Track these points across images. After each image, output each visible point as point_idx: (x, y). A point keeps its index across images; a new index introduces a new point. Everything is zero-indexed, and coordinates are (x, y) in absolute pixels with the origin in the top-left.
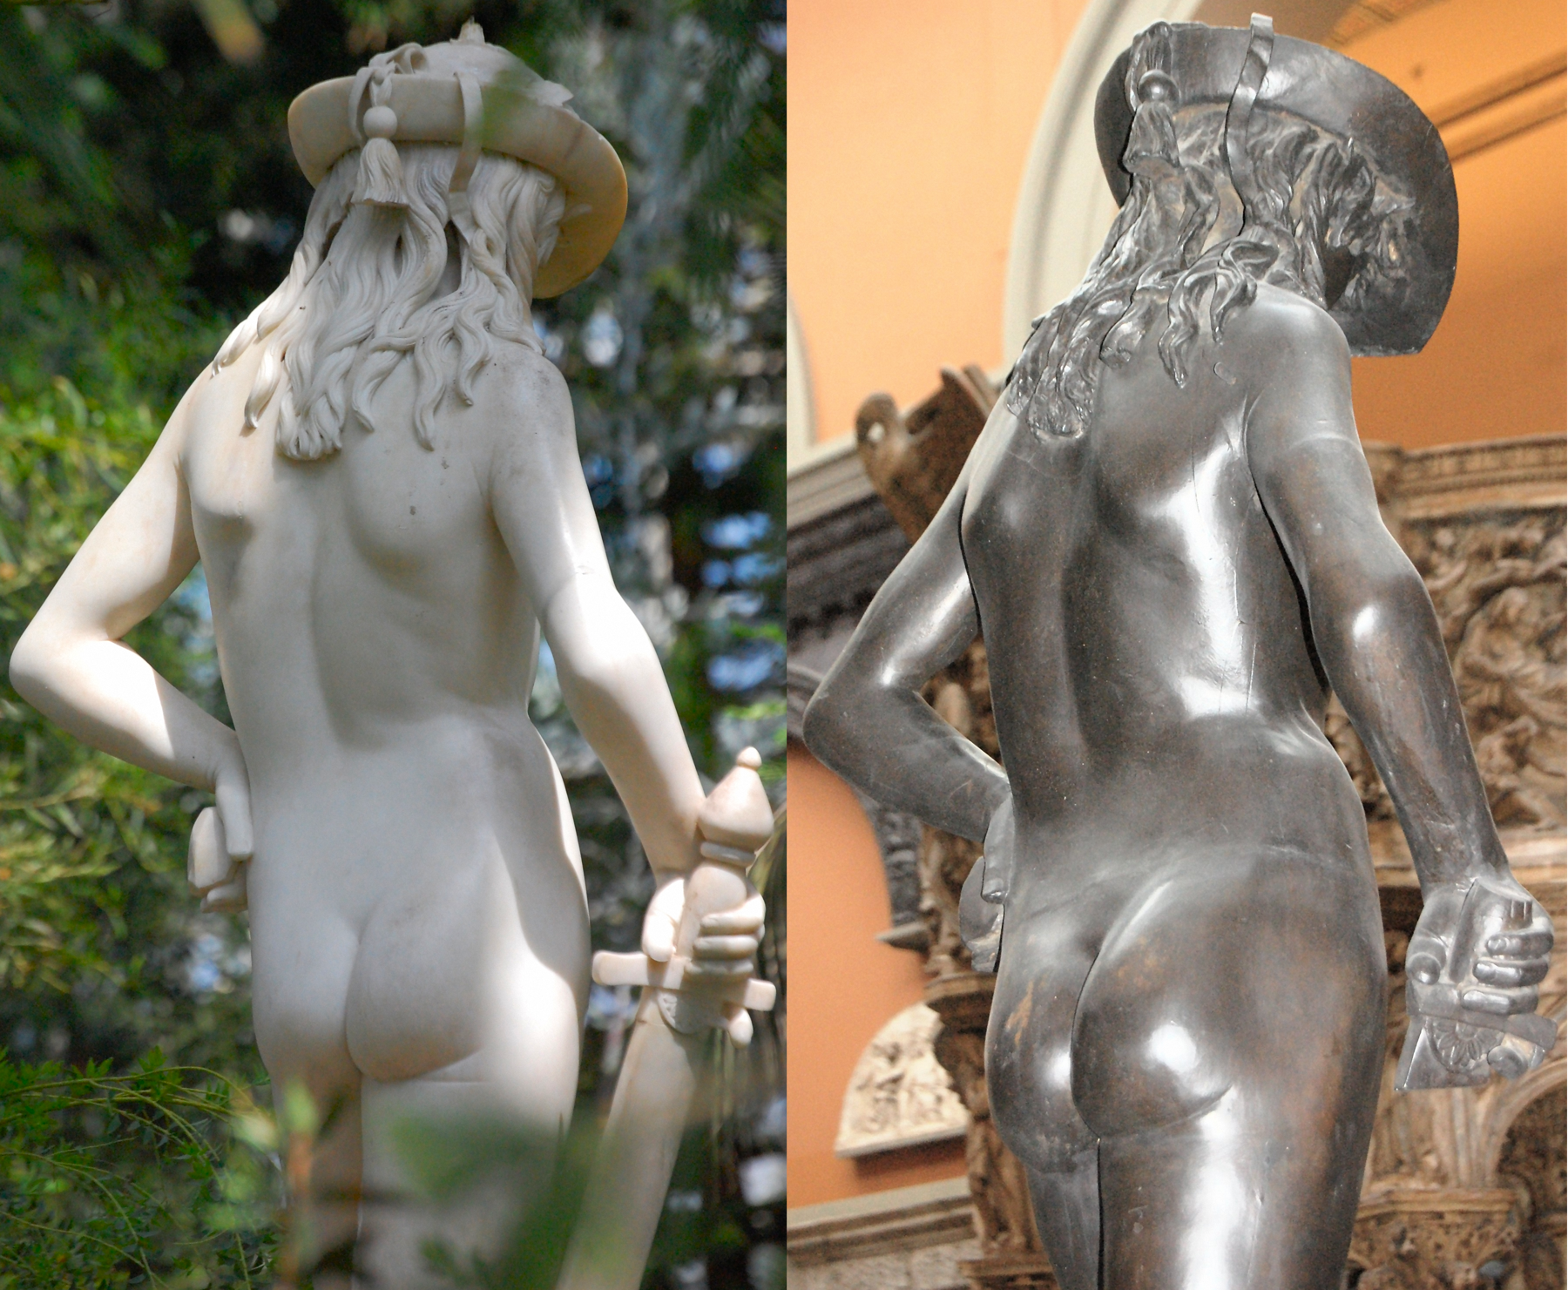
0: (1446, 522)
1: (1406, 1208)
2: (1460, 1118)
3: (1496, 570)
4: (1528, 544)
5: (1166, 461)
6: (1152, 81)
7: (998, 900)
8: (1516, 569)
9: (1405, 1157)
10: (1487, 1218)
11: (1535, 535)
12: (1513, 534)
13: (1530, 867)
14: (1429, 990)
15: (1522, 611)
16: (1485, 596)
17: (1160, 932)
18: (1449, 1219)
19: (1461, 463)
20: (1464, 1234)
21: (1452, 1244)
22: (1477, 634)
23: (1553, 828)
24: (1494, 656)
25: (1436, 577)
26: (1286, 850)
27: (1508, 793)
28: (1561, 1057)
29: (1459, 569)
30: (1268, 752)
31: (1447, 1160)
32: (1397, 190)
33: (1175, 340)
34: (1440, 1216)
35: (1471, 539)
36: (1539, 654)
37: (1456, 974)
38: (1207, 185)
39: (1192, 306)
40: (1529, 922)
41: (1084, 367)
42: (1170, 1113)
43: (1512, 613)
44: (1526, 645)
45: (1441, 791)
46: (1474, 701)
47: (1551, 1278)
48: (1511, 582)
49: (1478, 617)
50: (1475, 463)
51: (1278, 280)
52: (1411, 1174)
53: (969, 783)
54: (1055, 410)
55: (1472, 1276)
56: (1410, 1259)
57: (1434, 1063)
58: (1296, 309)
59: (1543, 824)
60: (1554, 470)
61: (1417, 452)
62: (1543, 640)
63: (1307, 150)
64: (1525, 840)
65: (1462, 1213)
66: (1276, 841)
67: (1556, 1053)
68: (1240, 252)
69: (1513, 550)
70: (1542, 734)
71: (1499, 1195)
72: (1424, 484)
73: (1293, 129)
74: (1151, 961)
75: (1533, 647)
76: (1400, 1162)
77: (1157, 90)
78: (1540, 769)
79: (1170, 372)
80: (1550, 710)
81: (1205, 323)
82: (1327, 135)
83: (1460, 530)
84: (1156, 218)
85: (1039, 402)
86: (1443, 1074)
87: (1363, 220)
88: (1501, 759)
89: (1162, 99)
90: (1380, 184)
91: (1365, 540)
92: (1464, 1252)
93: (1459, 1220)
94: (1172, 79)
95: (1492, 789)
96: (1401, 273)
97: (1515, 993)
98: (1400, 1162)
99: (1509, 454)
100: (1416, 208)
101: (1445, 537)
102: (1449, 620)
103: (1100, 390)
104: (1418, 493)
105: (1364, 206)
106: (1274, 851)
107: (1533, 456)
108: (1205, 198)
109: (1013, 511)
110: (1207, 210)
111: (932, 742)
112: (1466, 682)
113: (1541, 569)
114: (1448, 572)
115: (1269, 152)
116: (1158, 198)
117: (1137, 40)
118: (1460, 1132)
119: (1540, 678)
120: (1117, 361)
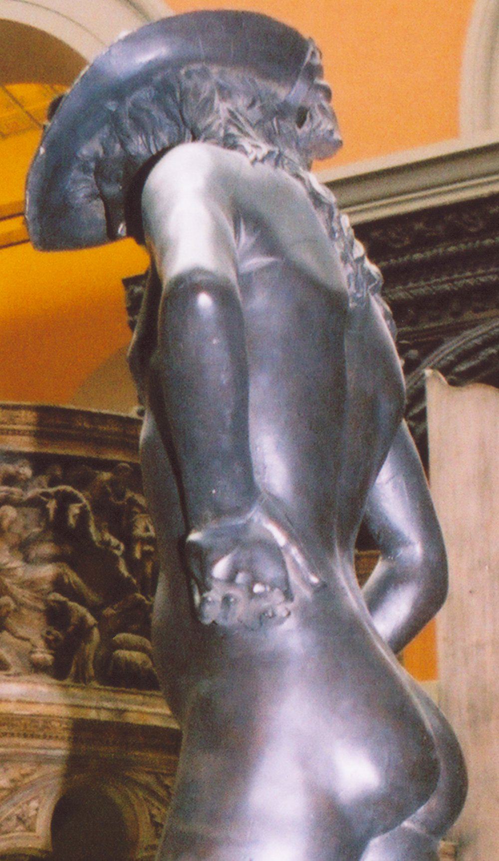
8: (12, 493)
12: (11, 469)
15: (12, 522)
23: (18, 675)
28: (7, 832)
36: (21, 556)
44: (11, 549)
59: (11, 672)
78: (13, 634)
80: (25, 595)
99: (17, 413)
119: (20, 572)
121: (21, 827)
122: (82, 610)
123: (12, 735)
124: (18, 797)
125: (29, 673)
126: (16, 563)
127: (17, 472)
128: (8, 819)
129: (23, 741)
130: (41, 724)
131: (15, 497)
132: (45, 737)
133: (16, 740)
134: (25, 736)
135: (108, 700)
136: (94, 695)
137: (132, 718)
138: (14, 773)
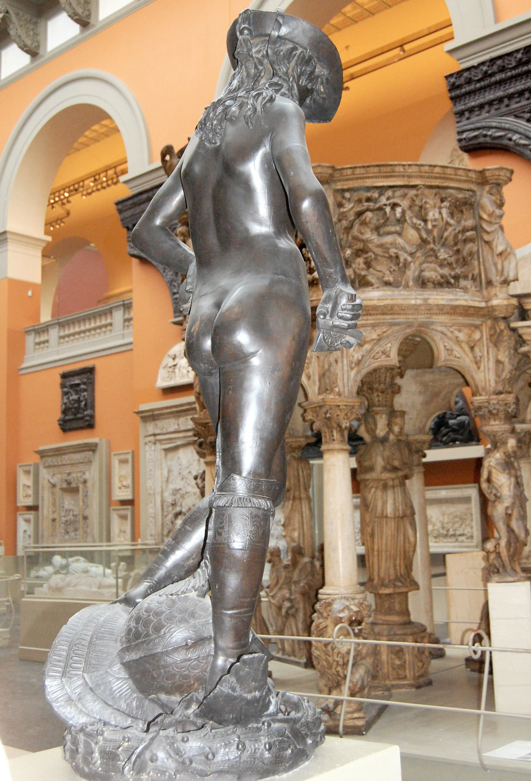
0: (348, 190)
1: (328, 403)
2: (346, 376)
3: (363, 206)
4: (373, 198)
5: (246, 152)
6: (244, 28)
7: (191, 292)
9: (329, 388)
10: (353, 407)
11: (376, 195)
12: (369, 194)
13: (370, 300)
14: (323, 320)
15: (371, 219)
16: (360, 214)
17: (240, 302)
18: (341, 407)
19: (353, 171)
20: (346, 411)
21: (342, 415)
22: (356, 226)
23: (378, 288)
24: (362, 233)
25: (344, 208)
27: (365, 276)
29: (351, 205)
30: (276, 246)
31: (341, 389)
32: (323, 68)
33: (249, 113)
34: (339, 406)
35: (356, 196)
36: (376, 233)
37: (332, 316)
38: (261, 63)
40: (355, 300)
41: (220, 122)
42: (242, 357)
43: (368, 219)
46: (355, 247)
47: (373, 427)
48: (368, 210)
49: (357, 220)
50: (358, 171)
51: (283, 95)
52: (330, 394)
53: (183, 256)
54: (211, 136)
55: (348, 424)
56: (329, 419)
57: (324, 343)
58: (288, 104)
59: (375, 286)
60: (382, 174)
61: (339, 167)
62: (377, 229)
63: (294, 53)
64: (369, 291)
65: (346, 405)
66: (277, 274)
67: (376, 357)
68: (271, 85)
69: (368, 200)
70: (376, 259)
71: (357, 400)
72: (341, 178)
73: (290, 46)
74: (236, 310)
75: (374, 231)
76: (327, 390)
77: (246, 32)
78: (374, 269)
79: (247, 124)
80: (379, 251)
81: (259, 108)
83: (352, 193)
84: (245, 74)
85: (205, 133)
86: (327, 347)
87: (312, 78)
88: (362, 266)
89: (247, 35)
90: (318, 66)
91: (307, 177)
92: (346, 417)
93: (344, 407)
94: (251, 28)
95: (360, 275)
96: (324, 96)
97: (350, 322)
98: (327, 390)
99: (369, 169)
100: (329, 74)
101: (347, 195)
102: (348, 222)
103: (225, 129)
104: (340, 180)
105: (312, 72)
106: (276, 277)
107: (376, 169)
108: (261, 68)
109: (197, 168)
110: (261, 72)
111: (172, 243)
112: (353, 241)
113: (377, 206)
114: (348, 206)
115: (282, 53)
116: (245, 67)
117: (240, 15)
118: (346, 381)
119: (376, 241)
120: (231, 120)
121: (384, 356)
122: (406, 255)
123: (377, 314)
124: (381, 343)
125: (383, 286)
126: (374, 237)
127: (371, 196)
128: (378, 353)
129: (382, 317)
130: (389, 308)
131: (371, 207)
132: (392, 314)
133: (379, 317)
134: (383, 314)
135: (420, 295)
136: (413, 293)
137: (430, 302)
138: (379, 331)
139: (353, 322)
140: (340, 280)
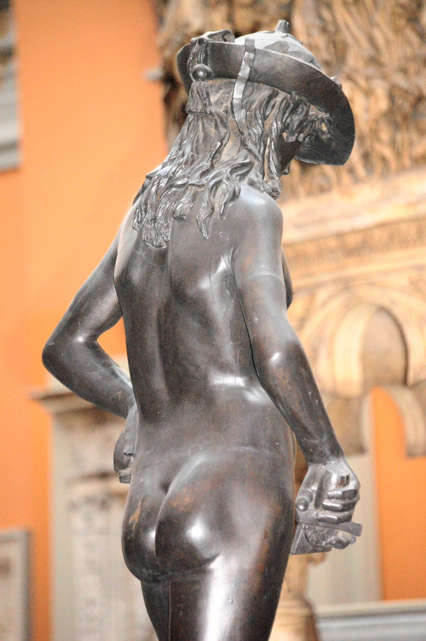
7: (130, 455)
26: (247, 448)
39: (212, 197)
45: (310, 428)
57: (306, 543)
63: (272, 103)
66: (243, 444)
82: (283, 93)
86: (311, 548)
97: (341, 515)
100: (331, 115)
106: (242, 449)
109: (137, 275)
139: (346, 513)
140: (328, 453)
